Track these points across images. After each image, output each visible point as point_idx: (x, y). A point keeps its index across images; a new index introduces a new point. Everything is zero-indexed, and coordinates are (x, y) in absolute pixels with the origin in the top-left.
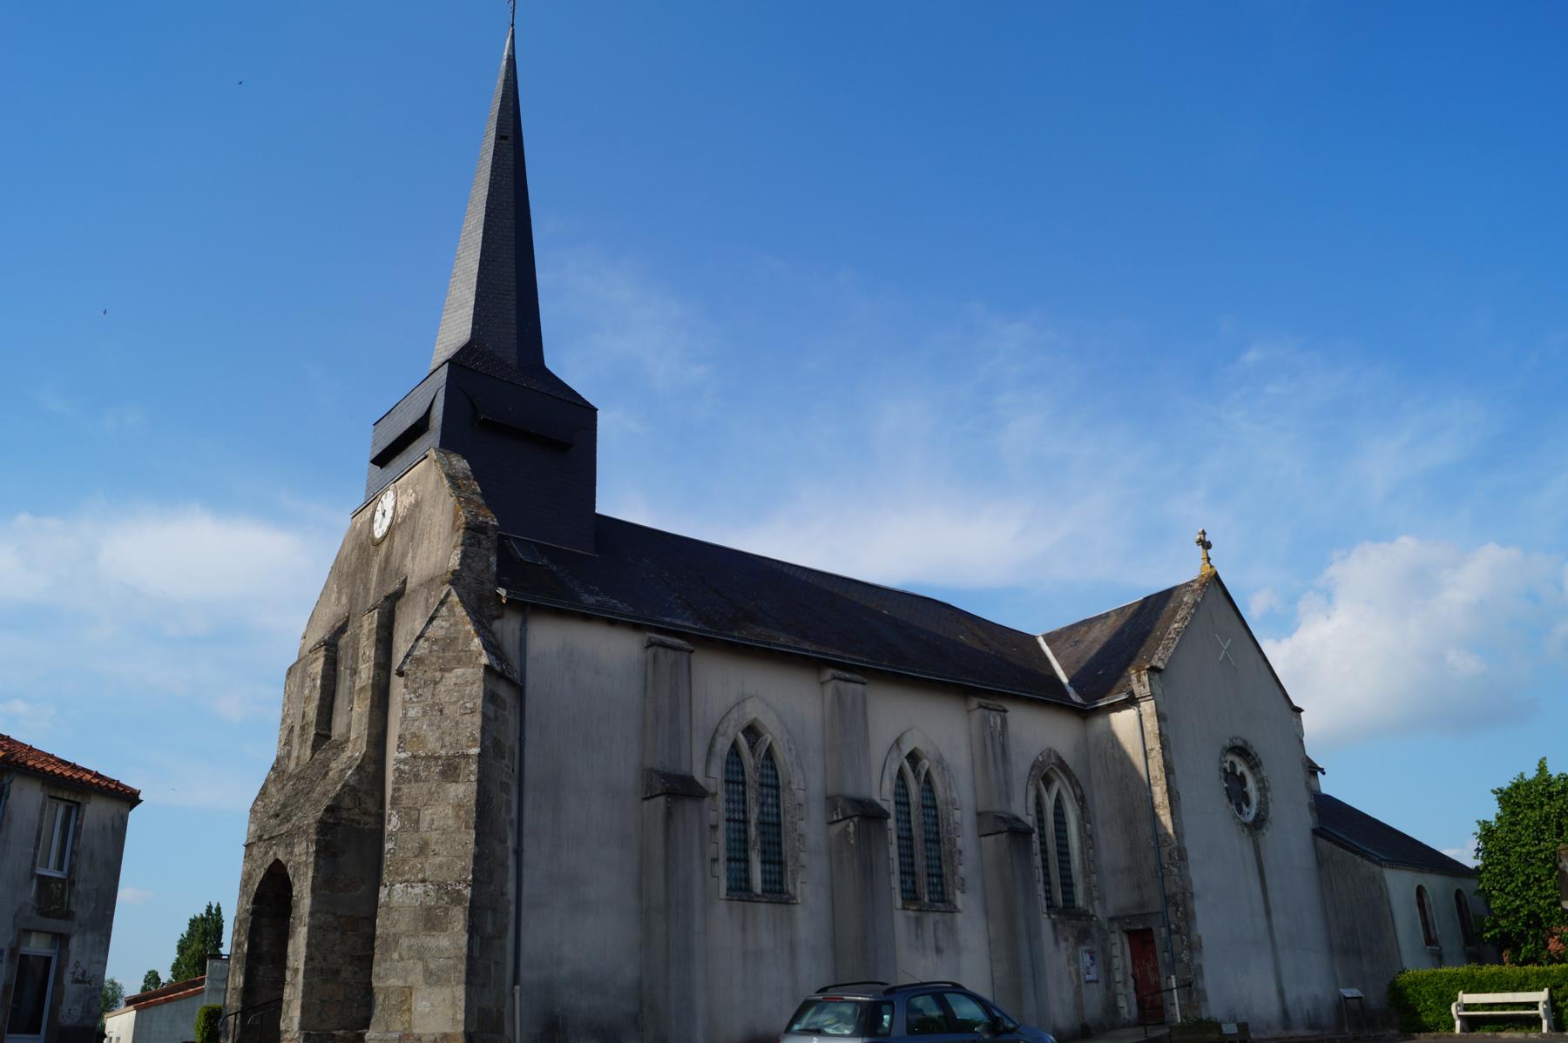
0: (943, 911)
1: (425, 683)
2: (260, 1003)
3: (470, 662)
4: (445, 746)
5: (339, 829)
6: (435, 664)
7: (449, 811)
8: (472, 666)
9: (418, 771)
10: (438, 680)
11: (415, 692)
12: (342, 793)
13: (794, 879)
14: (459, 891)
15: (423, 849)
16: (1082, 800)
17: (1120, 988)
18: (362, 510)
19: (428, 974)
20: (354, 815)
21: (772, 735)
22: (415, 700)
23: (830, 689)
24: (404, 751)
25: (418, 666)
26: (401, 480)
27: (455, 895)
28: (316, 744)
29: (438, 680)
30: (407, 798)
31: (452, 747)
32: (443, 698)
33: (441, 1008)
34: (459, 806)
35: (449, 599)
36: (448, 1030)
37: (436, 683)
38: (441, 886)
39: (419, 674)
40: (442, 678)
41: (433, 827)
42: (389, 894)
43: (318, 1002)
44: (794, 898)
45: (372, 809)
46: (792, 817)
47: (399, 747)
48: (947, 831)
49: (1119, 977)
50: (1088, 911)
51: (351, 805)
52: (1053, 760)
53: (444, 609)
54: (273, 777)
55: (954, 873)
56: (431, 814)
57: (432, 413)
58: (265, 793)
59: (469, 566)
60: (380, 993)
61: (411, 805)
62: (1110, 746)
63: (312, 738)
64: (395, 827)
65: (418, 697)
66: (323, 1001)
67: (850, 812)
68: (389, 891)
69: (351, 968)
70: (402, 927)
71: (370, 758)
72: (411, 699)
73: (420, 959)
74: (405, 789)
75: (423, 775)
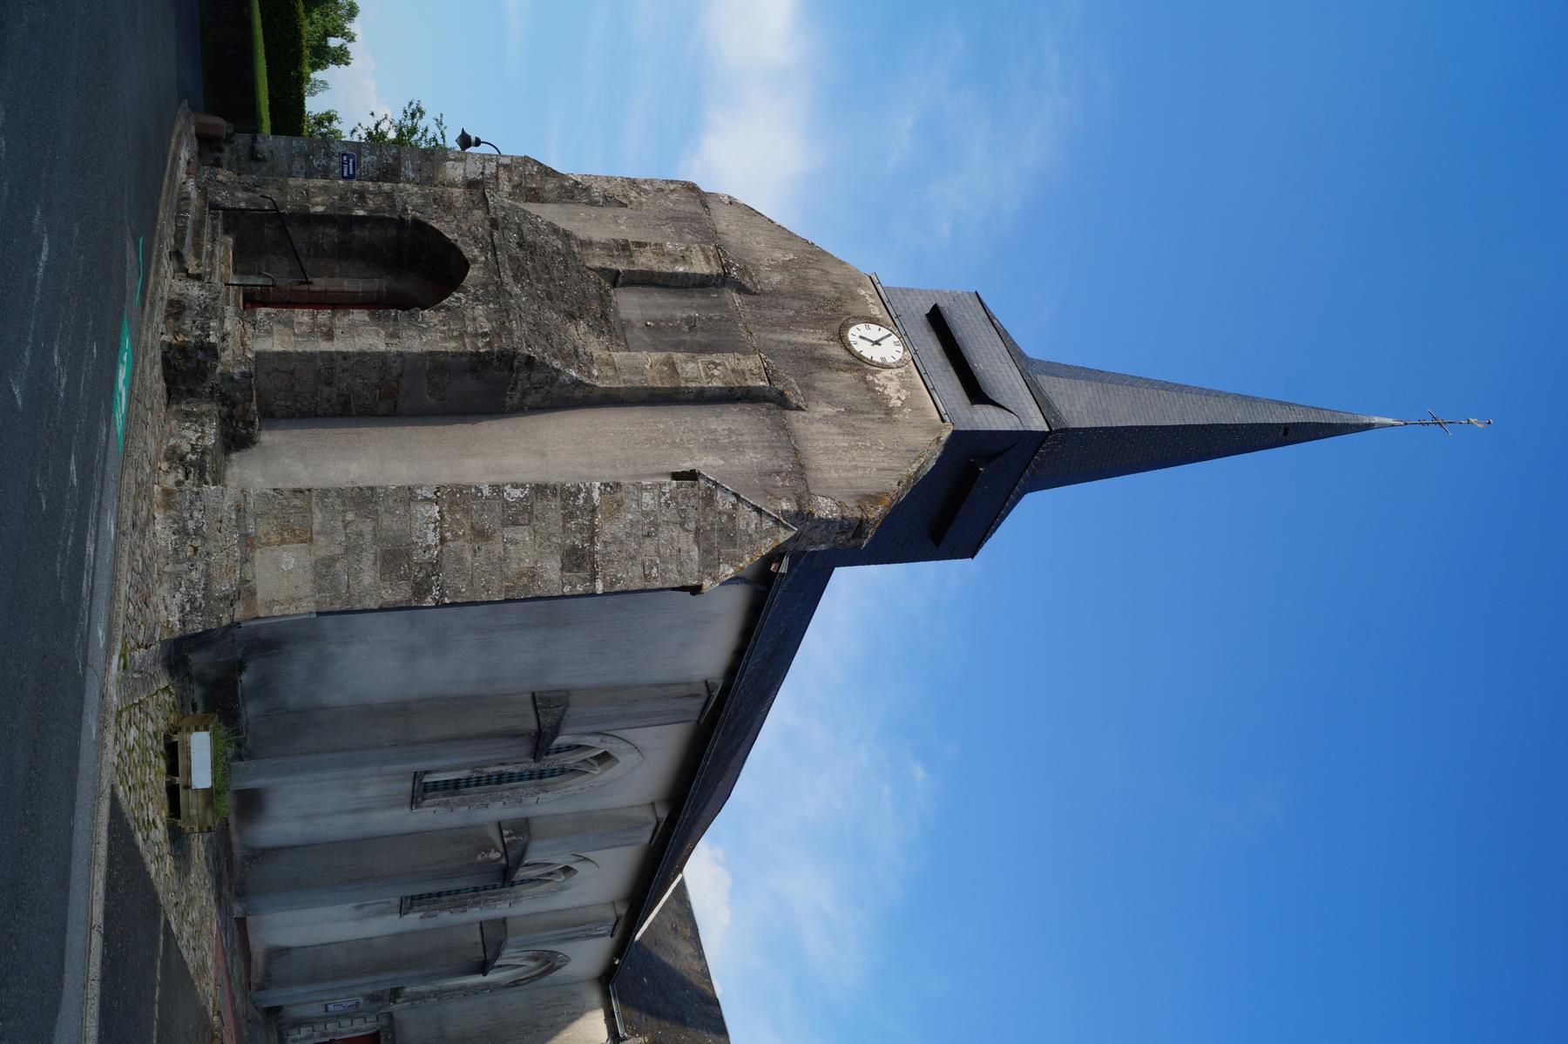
0: (401, 906)
1: (683, 510)
2: (290, 232)
3: (706, 567)
4: (606, 547)
5: (506, 372)
6: (705, 521)
7: (527, 563)
8: (701, 569)
9: (577, 517)
10: (686, 526)
11: (672, 498)
12: (550, 370)
13: (438, 804)
14: (430, 591)
15: (481, 534)
16: (516, 984)
17: (319, 1028)
18: (877, 290)
19: (328, 562)
20: (522, 384)
21: (599, 774)
22: (662, 500)
23: (647, 815)
24: (601, 494)
25: (703, 498)
26: (916, 371)
27: (426, 587)
28: (606, 272)
29: (686, 526)
30: (544, 507)
31: (604, 556)
32: (664, 534)
33: (286, 583)
34: (533, 575)
35: (782, 530)
36: (259, 596)
37: (682, 525)
38: (436, 566)
39: (693, 501)
40: (687, 531)
41: (508, 545)
42: (426, 499)
43: (292, 368)
44: (417, 807)
45: (529, 400)
46: (508, 797)
47: (606, 485)
48: (487, 900)
49: (331, 1027)
50: (399, 997)
51: (534, 380)
52: (557, 964)
53: (771, 524)
54: (567, 184)
55: (442, 909)
56: (524, 541)
57: (991, 407)
58: (547, 175)
59: (817, 527)
60: (303, 500)
61: (535, 513)
62: (571, 1011)
63: (614, 267)
64: (509, 494)
65: (666, 502)
66: (293, 371)
67: (511, 854)
68: (429, 499)
69: (335, 396)
70: (386, 520)
71: (591, 392)
72: (664, 494)
73: (347, 549)
74: (555, 503)
75: (572, 525)
